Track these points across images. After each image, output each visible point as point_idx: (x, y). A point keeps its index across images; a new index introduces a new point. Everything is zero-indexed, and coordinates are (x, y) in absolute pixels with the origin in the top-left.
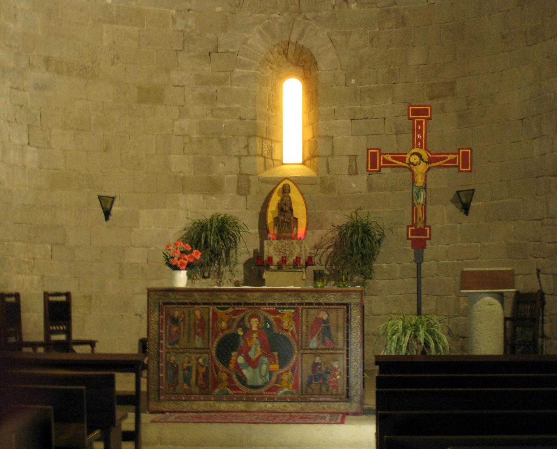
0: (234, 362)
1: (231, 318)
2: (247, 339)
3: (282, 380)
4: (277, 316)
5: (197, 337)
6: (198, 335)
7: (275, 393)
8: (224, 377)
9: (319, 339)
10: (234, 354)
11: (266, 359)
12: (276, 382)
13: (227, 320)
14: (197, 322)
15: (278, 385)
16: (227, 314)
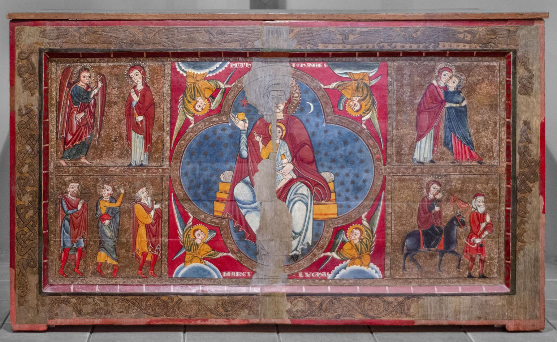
0: (225, 196)
1: (218, 90)
2: (258, 139)
3: (343, 243)
4: (333, 85)
5: (133, 133)
6: (136, 132)
7: (330, 276)
8: (202, 236)
9: (436, 139)
10: (227, 176)
11: (304, 190)
12: (329, 248)
13: (208, 94)
14: (136, 99)
15: (334, 255)
16: (209, 79)
